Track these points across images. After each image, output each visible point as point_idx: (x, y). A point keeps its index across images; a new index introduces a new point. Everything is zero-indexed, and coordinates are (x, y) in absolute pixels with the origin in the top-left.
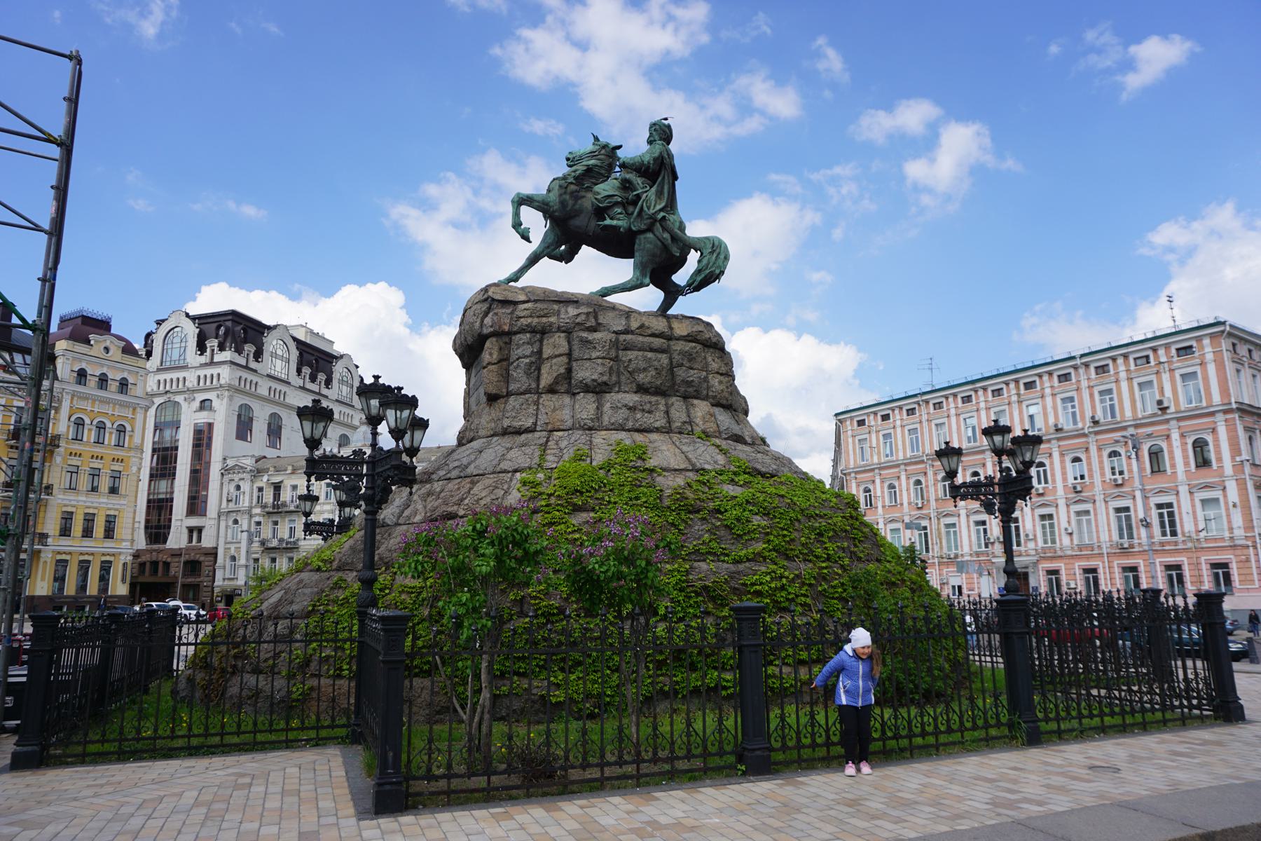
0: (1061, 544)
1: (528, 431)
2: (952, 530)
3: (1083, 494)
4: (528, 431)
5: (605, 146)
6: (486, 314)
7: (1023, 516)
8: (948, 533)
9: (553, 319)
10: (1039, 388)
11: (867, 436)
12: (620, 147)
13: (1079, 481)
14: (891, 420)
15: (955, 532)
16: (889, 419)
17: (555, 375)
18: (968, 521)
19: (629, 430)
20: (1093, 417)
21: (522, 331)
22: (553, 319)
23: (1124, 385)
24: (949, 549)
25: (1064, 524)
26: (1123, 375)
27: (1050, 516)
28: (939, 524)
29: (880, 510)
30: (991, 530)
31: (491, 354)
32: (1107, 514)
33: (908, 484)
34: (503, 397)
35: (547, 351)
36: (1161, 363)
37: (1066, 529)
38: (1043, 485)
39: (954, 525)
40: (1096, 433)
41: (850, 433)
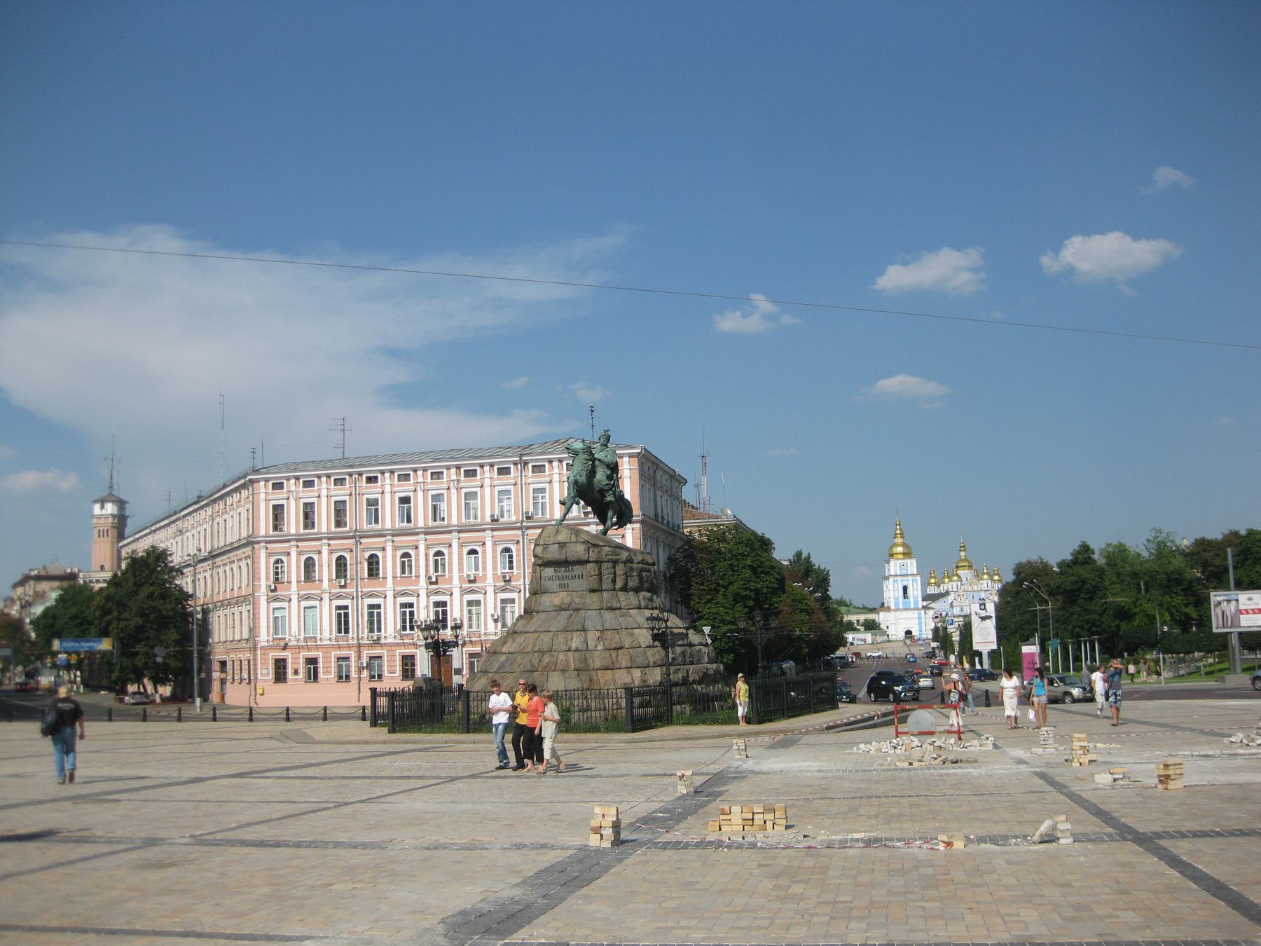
0: (486, 629)
1: (620, 608)
2: (375, 611)
3: (512, 583)
4: (620, 608)
6: (588, 549)
7: (451, 601)
8: (371, 615)
10: (479, 477)
11: (284, 502)
13: (507, 570)
14: (316, 488)
15: (379, 614)
16: (313, 486)
18: (395, 603)
20: (527, 513)
21: (608, 561)
22: (619, 557)
24: (371, 630)
25: (490, 610)
27: (478, 603)
28: (362, 604)
29: (294, 585)
30: (418, 612)
31: (594, 571)
33: (330, 559)
35: (618, 573)
37: (493, 615)
38: (474, 572)
39: (378, 606)
40: (528, 528)
41: (262, 496)
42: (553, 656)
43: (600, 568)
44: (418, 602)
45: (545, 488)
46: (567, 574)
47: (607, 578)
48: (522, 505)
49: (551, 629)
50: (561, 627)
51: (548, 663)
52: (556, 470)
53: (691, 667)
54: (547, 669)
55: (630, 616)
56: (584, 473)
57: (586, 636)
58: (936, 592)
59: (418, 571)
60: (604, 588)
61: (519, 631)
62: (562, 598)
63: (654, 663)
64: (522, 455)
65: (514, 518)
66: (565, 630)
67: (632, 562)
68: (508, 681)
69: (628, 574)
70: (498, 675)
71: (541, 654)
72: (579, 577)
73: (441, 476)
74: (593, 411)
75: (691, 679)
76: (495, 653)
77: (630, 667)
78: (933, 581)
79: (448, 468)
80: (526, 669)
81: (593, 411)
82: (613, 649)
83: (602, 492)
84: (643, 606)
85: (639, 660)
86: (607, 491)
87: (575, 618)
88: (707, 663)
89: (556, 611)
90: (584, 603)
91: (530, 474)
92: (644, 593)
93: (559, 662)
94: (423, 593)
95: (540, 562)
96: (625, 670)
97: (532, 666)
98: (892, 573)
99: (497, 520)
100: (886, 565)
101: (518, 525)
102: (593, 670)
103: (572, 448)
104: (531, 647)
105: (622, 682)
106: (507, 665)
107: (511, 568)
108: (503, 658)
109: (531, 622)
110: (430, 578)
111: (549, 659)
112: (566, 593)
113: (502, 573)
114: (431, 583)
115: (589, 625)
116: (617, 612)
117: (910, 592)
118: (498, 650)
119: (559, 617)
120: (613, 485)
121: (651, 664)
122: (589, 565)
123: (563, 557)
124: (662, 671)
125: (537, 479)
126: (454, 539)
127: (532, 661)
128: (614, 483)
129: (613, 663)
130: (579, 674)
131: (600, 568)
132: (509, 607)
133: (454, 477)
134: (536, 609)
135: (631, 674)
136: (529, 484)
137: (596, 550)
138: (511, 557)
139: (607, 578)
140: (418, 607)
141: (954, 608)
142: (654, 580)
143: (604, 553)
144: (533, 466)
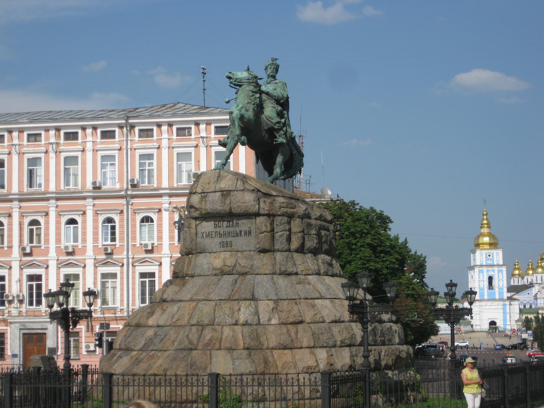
1: (297, 274)
3: (114, 257)
4: (297, 274)
5: (256, 77)
6: (259, 199)
7: (47, 274)
9: (295, 210)
10: (80, 140)
12: (260, 79)
13: (109, 242)
17: (300, 243)
19: (329, 276)
20: (132, 180)
21: (283, 215)
22: (295, 210)
23: (165, 152)
26: (165, 143)
30: (10, 286)
31: (266, 226)
32: (134, 278)
34: (271, 251)
36: (202, 137)
38: (72, 243)
40: (133, 197)
42: (214, 330)
43: (272, 223)
44: (10, 275)
45: (153, 154)
46: (231, 229)
47: (280, 234)
48: (127, 172)
49: (212, 297)
50: (224, 294)
51: (211, 340)
52: (165, 135)
53: (384, 348)
54: (210, 347)
55: (309, 284)
56: (251, 107)
57: (256, 307)
58: (520, 284)
59: (10, 241)
60: (276, 247)
61: (169, 299)
62: (223, 259)
63: (342, 342)
64: (128, 118)
65: (118, 186)
66: (230, 299)
67: (309, 218)
68: (160, 361)
69: (306, 232)
70: (144, 354)
71: (200, 328)
72: (245, 233)
73: (38, 138)
74: (204, 74)
75: (383, 363)
76: (138, 326)
77: (313, 347)
78: (517, 272)
79: (47, 130)
80: (183, 346)
81: (204, 74)
82: (291, 324)
83: (272, 132)
84: (322, 271)
85: (324, 338)
86: (278, 130)
87: (241, 284)
88: (398, 344)
89: (215, 275)
90: (252, 265)
91: (137, 138)
92: (322, 255)
93: (224, 337)
94: (16, 265)
95: (196, 214)
96: (308, 350)
97: (191, 343)
98: (478, 263)
99: (99, 188)
100: (472, 255)
101: (123, 193)
102: (268, 349)
103: (234, 77)
104: (186, 318)
105: (304, 365)
106: (157, 341)
107: (113, 239)
108: (150, 333)
109: (184, 289)
110: (24, 249)
111: (211, 335)
112: (229, 253)
113: (103, 245)
114: (26, 255)
115: (259, 293)
116: (293, 278)
117: (495, 283)
118: (142, 322)
119: (221, 283)
120: (284, 124)
121: (338, 343)
122: (259, 220)
123: (227, 208)
124: (351, 352)
125: (144, 144)
126: (52, 207)
127: (190, 336)
128: (285, 121)
129: (292, 341)
130: (250, 355)
131: (272, 223)
132: (110, 283)
133: (53, 140)
134: (190, 273)
135: (315, 355)
136: (135, 149)
137: (268, 201)
138: (113, 228)
139: (280, 234)
140: (10, 280)
141: (539, 300)
142: (333, 241)
143: (277, 205)
144: (141, 131)
